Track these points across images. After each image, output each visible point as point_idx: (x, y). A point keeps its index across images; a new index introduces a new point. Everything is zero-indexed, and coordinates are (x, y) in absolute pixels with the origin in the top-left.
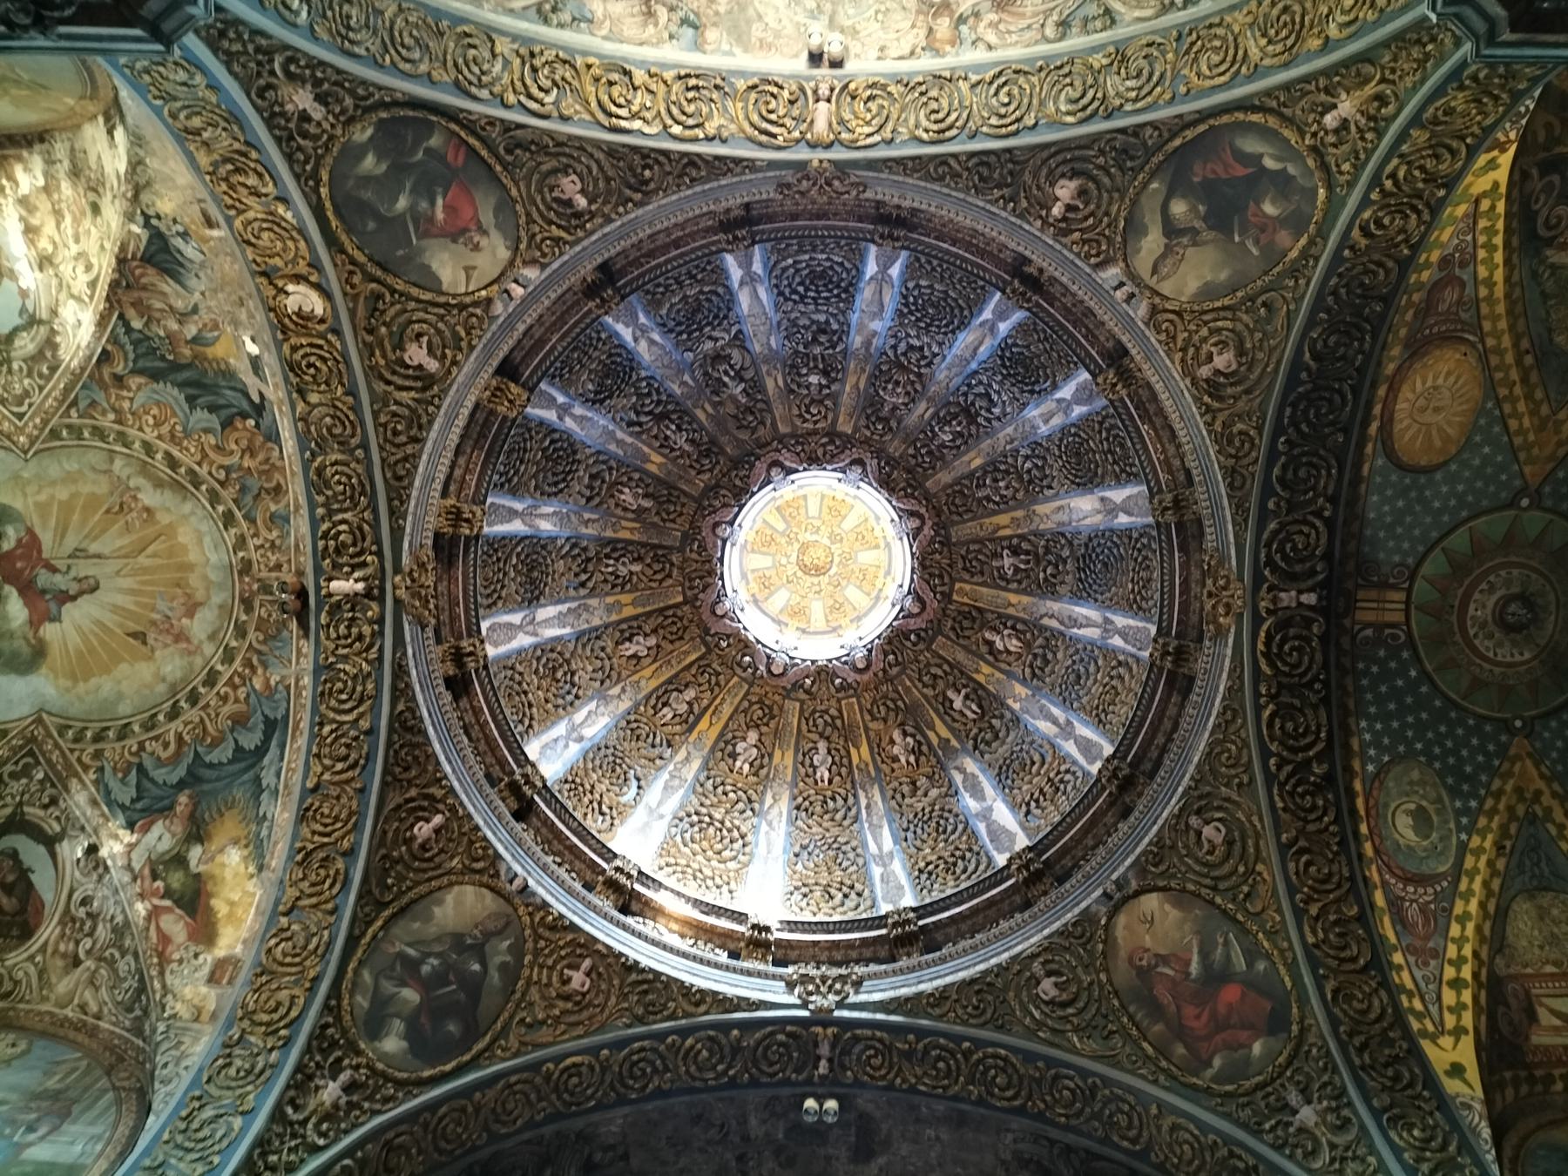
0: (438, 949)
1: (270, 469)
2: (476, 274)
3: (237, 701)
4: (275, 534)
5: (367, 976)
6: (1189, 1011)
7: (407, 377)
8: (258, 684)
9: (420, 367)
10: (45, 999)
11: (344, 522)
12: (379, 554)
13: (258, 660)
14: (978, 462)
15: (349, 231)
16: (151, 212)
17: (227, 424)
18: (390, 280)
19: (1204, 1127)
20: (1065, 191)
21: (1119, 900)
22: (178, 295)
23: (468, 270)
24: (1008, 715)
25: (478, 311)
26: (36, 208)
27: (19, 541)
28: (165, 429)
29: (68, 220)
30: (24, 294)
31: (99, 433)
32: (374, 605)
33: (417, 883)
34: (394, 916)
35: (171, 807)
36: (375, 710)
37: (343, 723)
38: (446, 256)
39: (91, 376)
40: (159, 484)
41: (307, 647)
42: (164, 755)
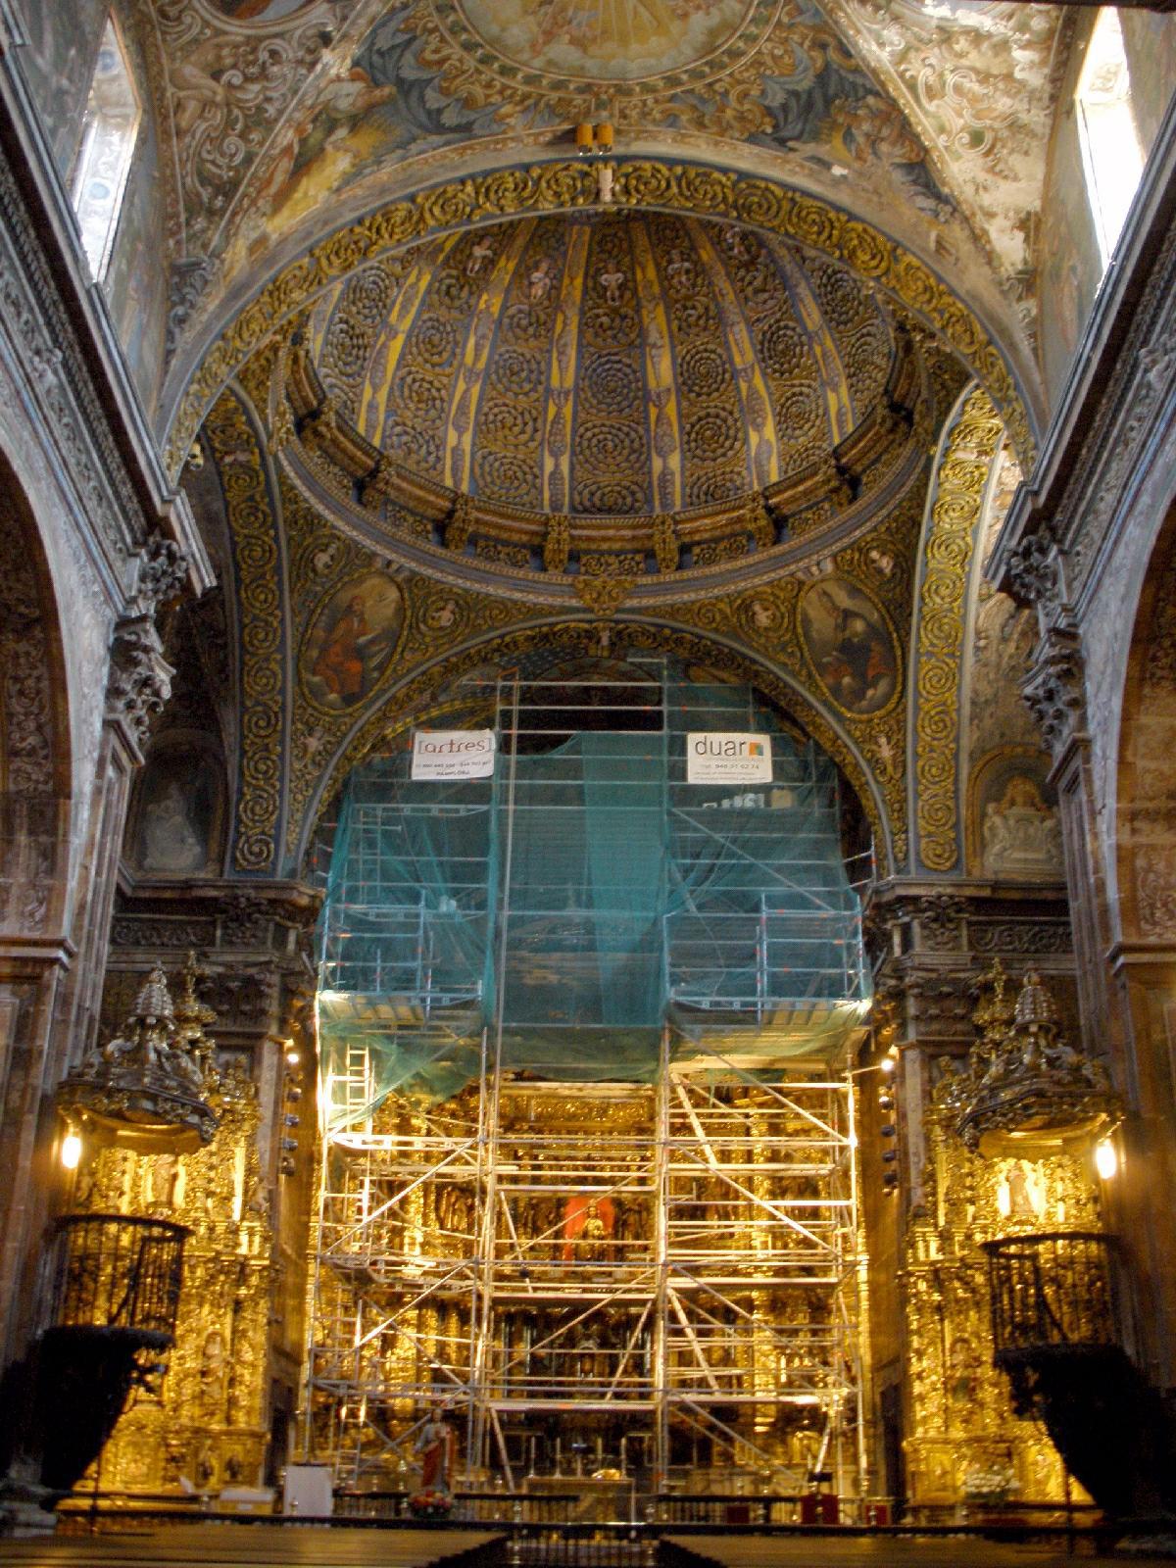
1: (724, 130)
3: (488, 96)
4: (658, 116)
6: (337, 649)
10: (172, 58)
13: (529, 105)
14: (704, 256)
17: (769, 111)
19: (282, 691)
20: (886, 564)
21: (387, 571)
22: (890, 155)
24: (473, 301)
26: (996, 55)
28: (769, 61)
29: (976, 87)
40: (713, 33)
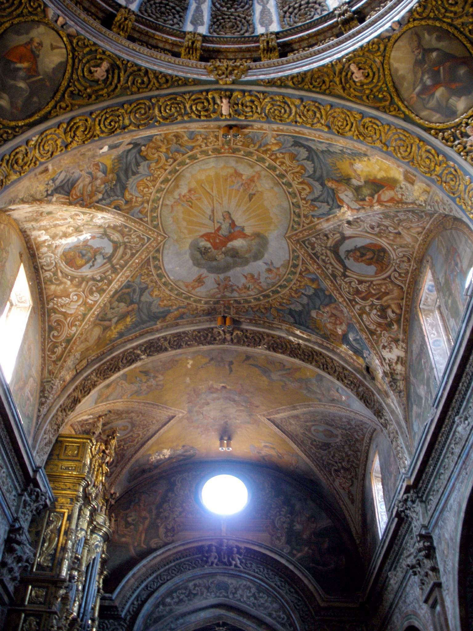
0: (419, 75)
1: (166, 139)
2: (54, 44)
4: (199, 138)
5: (424, 113)
7: (113, 77)
8: (275, 148)
9: (107, 71)
10: (413, 247)
11: (191, 107)
12: (207, 91)
15: (40, 110)
16: (45, 194)
17: (145, 158)
18: (62, 89)
22: (84, 180)
23: (53, 48)
25: (75, 41)
27: (206, 240)
28: (150, 184)
29: (57, 222)
30: (93, 237)
31: (154, 210)
32: (235, 94)
33: (385, 82)
34: (398, 95)
35: (333, 190)
36: (290, 96)
37: (296, 112)
38: (47, 60)
39: (128, 213)
40: (177, 186)
41: (257, 125)
42: (308, 190)
